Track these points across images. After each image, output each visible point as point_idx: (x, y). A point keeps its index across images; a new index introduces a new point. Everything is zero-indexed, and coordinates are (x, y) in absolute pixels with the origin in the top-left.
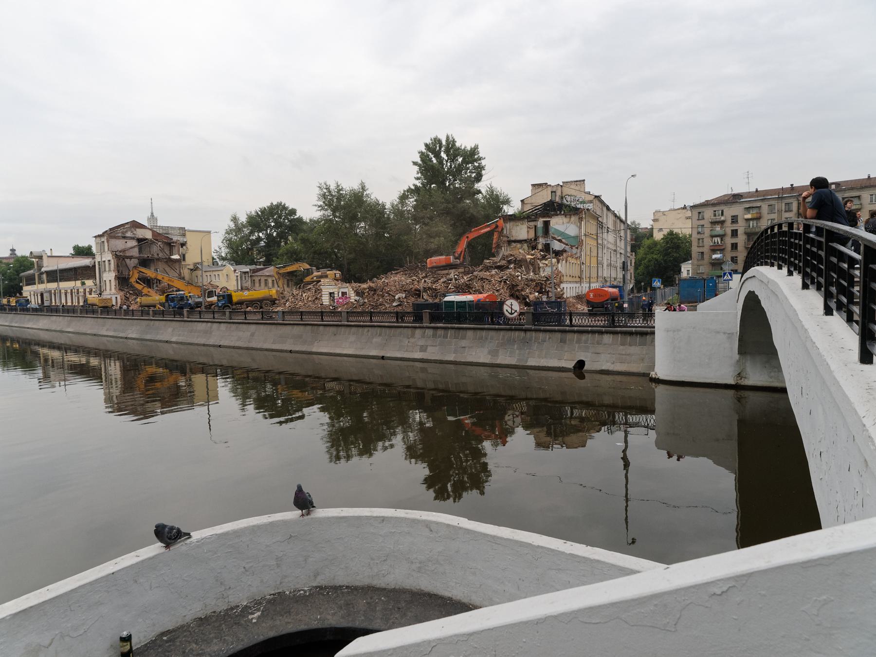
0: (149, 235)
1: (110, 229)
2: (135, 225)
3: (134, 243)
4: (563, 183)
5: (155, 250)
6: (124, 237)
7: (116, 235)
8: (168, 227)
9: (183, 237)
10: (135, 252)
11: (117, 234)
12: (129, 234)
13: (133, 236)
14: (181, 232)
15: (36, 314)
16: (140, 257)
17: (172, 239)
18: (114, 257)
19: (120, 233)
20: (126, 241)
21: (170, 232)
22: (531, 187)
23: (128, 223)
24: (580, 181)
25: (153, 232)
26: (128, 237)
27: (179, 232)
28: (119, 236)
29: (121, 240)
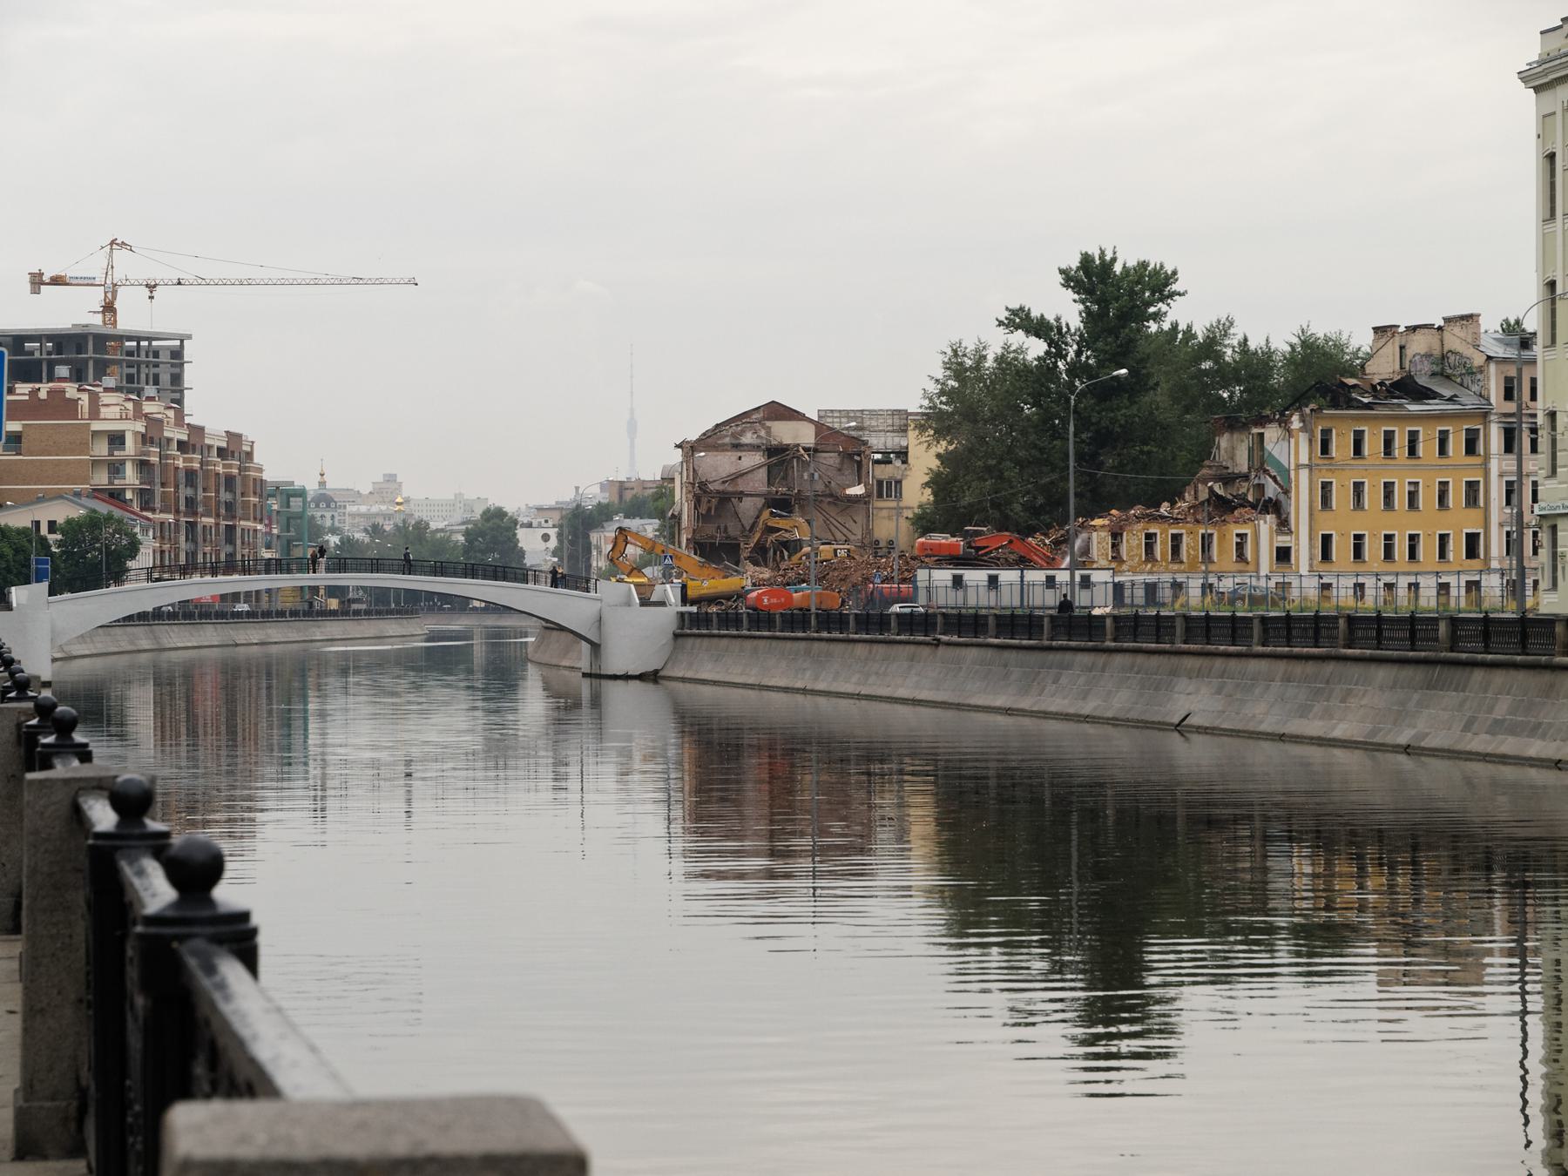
0: (805, 436)
1: (717, 425)
2: (777, 411)
3: (757, 459)
4: (1448, 320)
5: (805, 480)
6: (737, 446)
7: (719, 442)
8: (862, 411)
9: (901, 434)
10: (758, 482)
11: (720, 438)
12: (748, 438)
13: (758, 442)
14: (897, 422)
15: (800, 634)
16: (769, 493)
17: (865, 443)
18: (690, 496)
19: (727, 436)
20: (739, 454)
21: (867, 423)
22: (1372, 331)
23: (759, 408)
24: (1463, 318)
25: (819, 426)
26: (746, 445)
27: (890, 422)
28: (724, 445)
29: (729, 453)
